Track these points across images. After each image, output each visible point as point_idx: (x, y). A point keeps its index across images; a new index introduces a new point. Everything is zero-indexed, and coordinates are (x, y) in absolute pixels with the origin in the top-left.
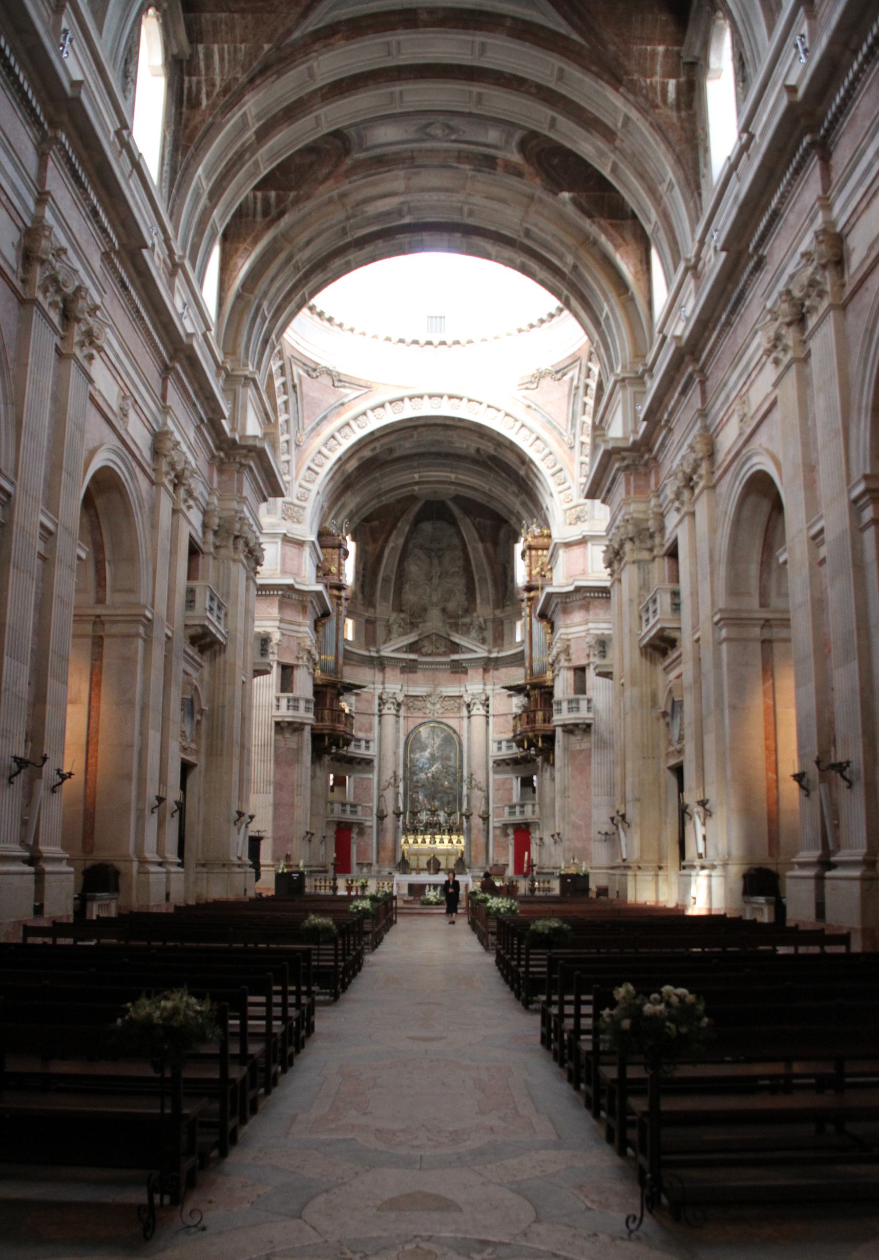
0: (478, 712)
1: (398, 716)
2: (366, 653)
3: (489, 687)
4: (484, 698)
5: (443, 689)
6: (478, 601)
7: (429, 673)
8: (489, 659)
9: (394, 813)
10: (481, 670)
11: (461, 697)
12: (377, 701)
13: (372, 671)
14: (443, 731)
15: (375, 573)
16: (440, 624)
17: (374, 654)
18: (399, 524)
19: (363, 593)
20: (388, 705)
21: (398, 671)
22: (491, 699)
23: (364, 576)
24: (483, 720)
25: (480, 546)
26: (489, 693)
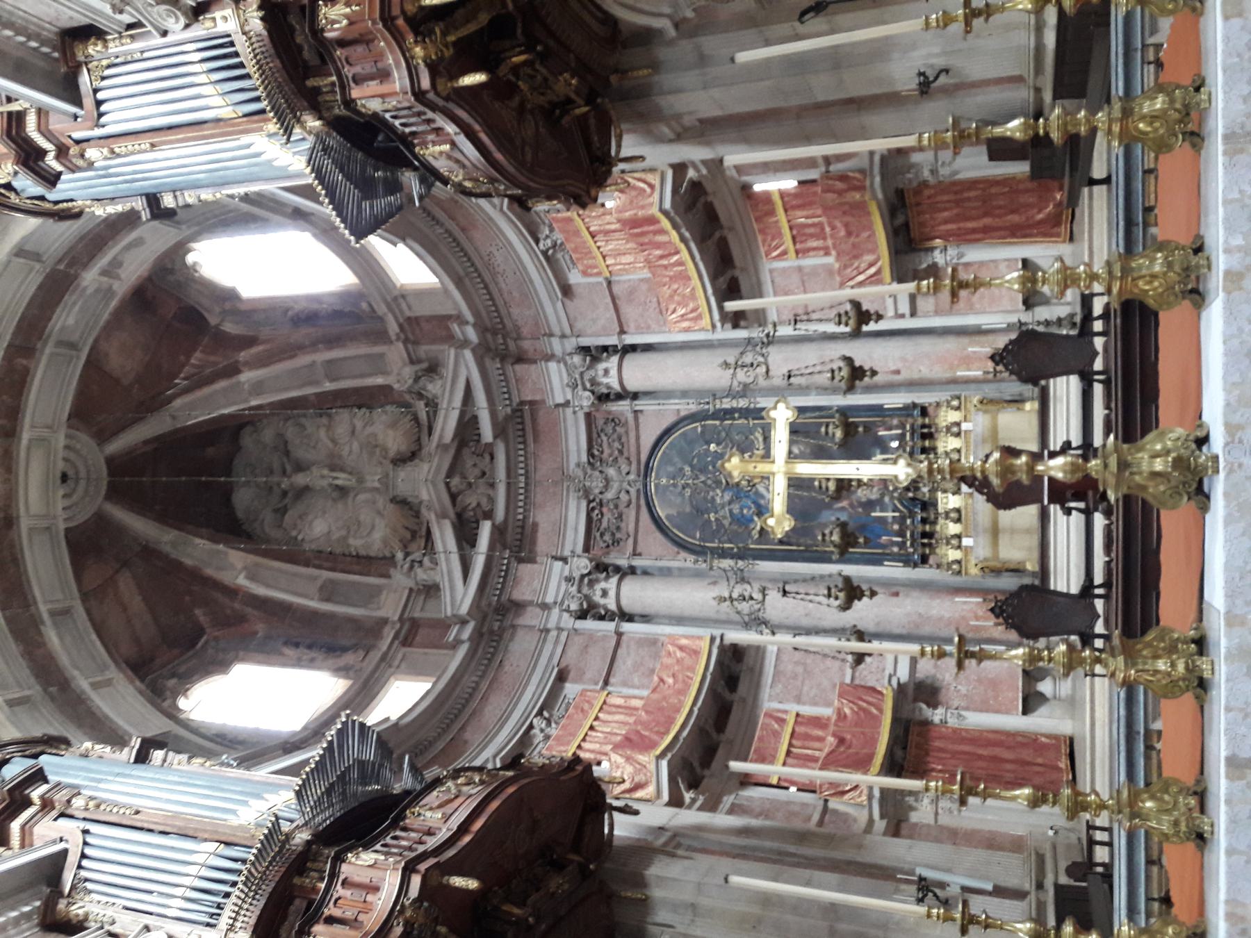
0: (614, 372)
1: (632, 571)
2: (463, 650)
3: (557, 346)
4: (577, 359)
5: (573, 460)
6: (380, 381)
7: (538, 496)
8: (483, 352)
9: (846, 606)
10: (518, 367)
11: (588, 416)
12: (589, 624)
13: (520, 633)
14: (666, 460)
15: (312, 618)
16: (426, 467)
17: (466, 635)
18: (188, 562)
19: (344, 650)
20: (597, 598)
21: (525, 569)
22: (585, 342)
23: (310, 647)
24: (630, 360)
25: (247, 376)
26: (571, 344)
